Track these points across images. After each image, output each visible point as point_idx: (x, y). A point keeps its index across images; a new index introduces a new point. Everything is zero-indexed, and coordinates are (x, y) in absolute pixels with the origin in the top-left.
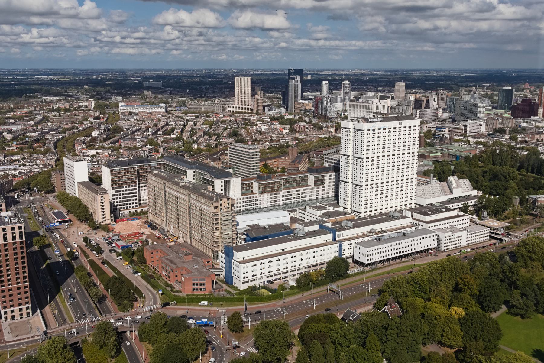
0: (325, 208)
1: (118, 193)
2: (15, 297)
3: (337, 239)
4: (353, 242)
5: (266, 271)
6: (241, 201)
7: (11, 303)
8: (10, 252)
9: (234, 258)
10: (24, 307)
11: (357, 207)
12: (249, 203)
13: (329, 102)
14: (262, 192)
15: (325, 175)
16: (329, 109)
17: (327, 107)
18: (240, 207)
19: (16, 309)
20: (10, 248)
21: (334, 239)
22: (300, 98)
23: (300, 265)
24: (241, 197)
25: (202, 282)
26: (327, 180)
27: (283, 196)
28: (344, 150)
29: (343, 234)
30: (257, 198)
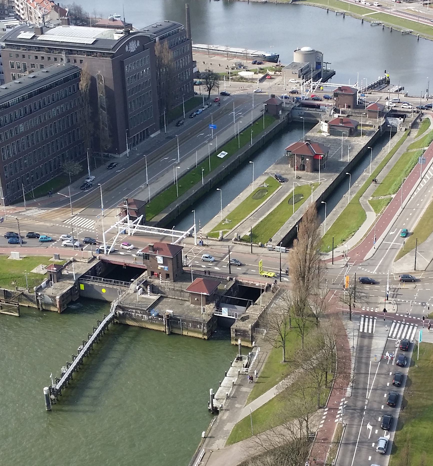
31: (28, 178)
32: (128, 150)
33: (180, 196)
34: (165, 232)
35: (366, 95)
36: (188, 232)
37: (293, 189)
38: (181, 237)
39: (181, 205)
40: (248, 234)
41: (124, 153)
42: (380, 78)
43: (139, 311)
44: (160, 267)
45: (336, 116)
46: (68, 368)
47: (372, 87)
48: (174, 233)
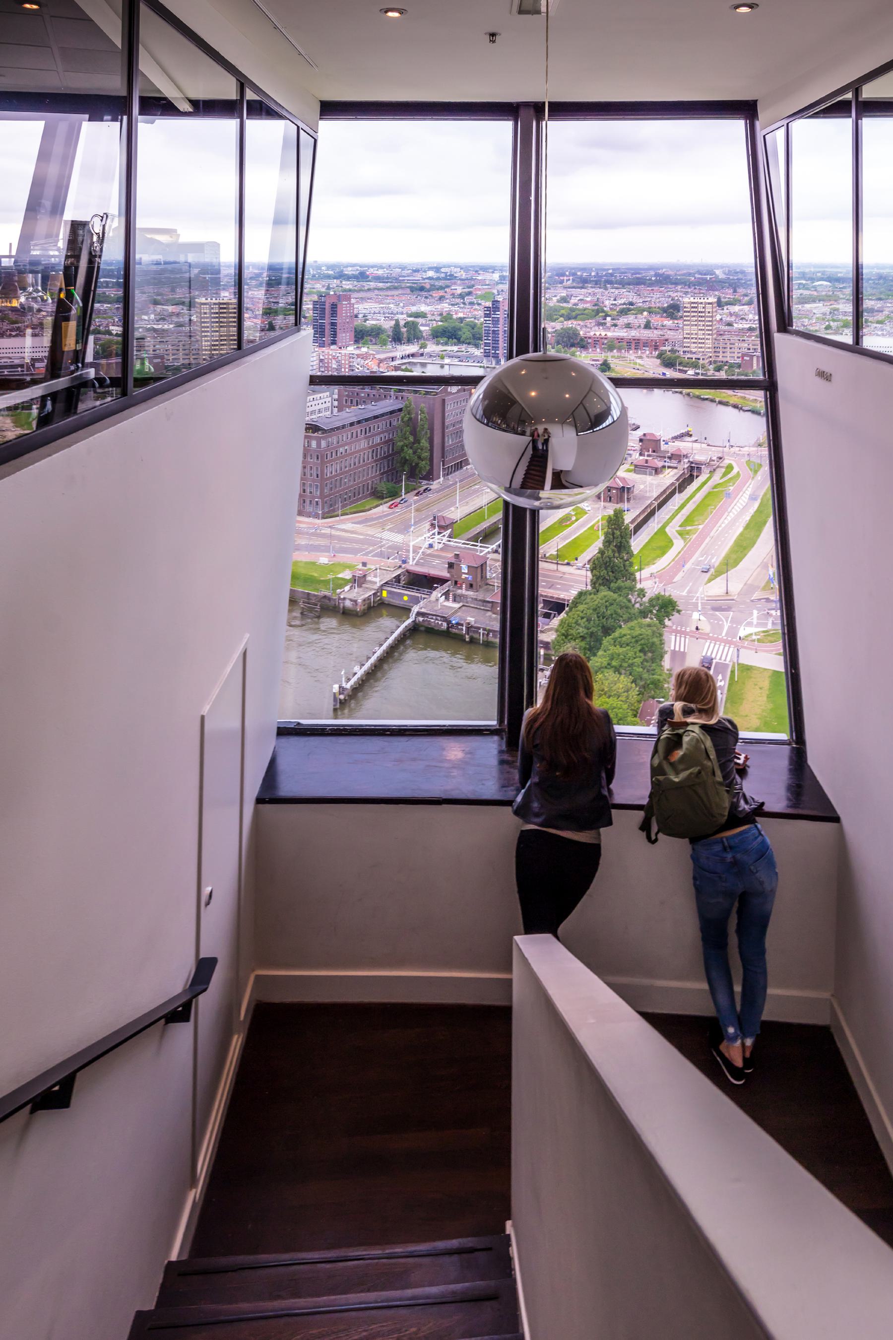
31: (346, 496)
32: (442, 479)
33: (488, 518)
34: (472, 545)
35: (669, 443)
37: (600, 517)
38: (487, 550)
39: (489, 527)
40: (555, 553)
41: (437, 481)
42: (683, 431)
43: (439, 618)
44: (464, 576)
45: (641, 458)
46: (361, 668)
47: (676, 438)
48: (481, 547)
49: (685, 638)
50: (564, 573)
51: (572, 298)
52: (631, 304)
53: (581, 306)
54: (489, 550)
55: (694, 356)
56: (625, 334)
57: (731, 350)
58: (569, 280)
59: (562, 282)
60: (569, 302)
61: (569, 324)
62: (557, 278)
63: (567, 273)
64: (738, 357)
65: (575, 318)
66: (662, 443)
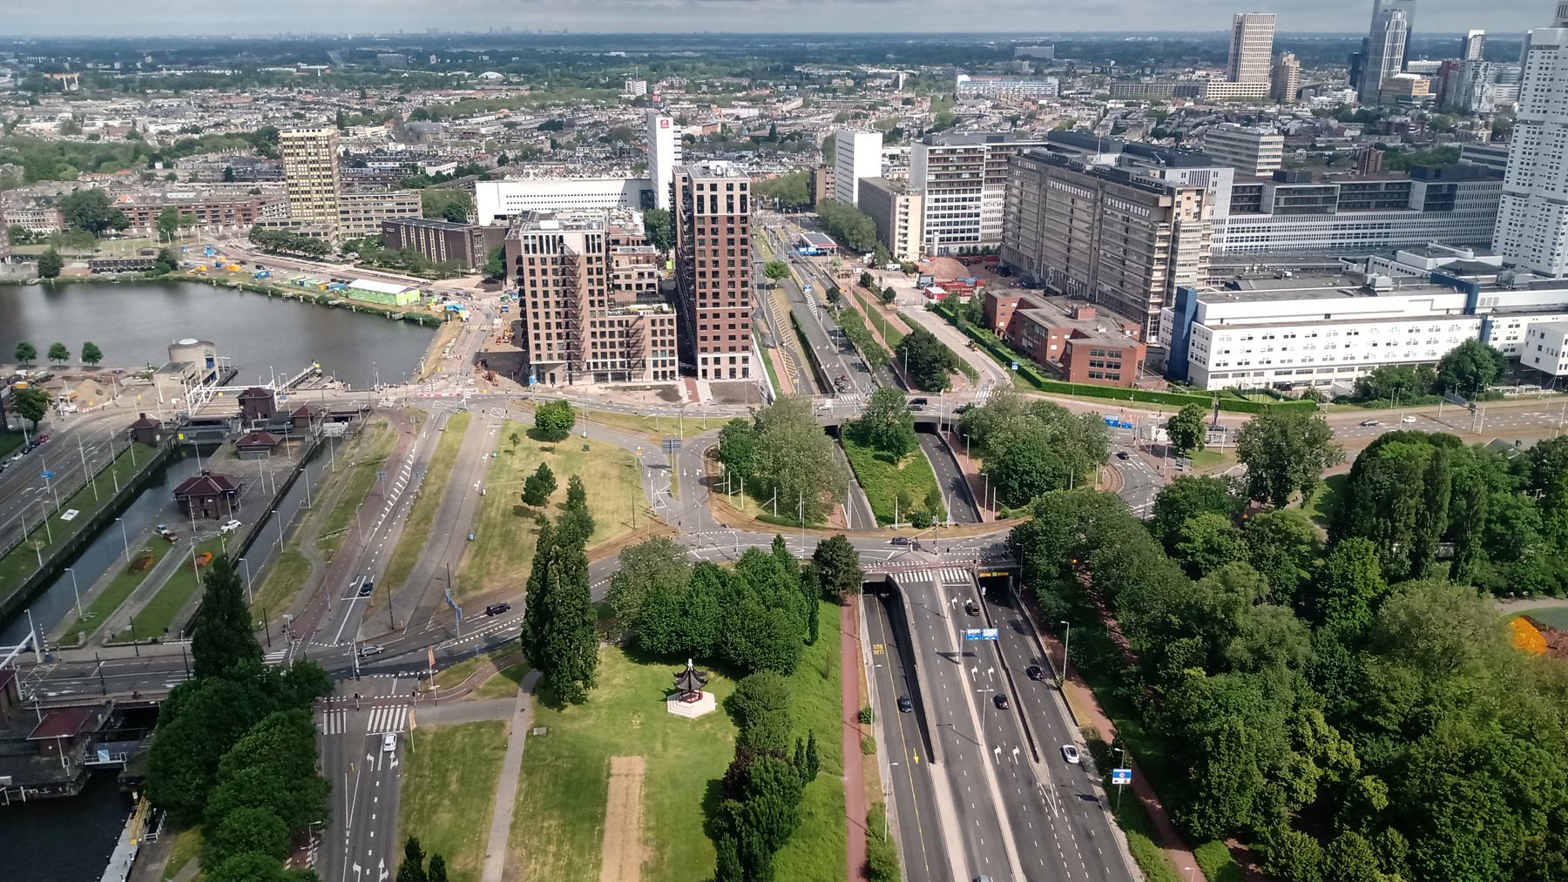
0: (1451, 254)
1: (941, 204)
2: (724, 333)
3: (1477, 311)
4: (1525, 321)
5: (1276, 358)
6: (1227, 226)
7: (717, 344)
8: (723, 236)
9: (1199, 318)
10: (739, 355)
11: (1544, 262)
12: (1245, 235)
13: (1482, 73)
14: (1284, 211)
15: (1459, 184)
16: (1478, 91)
17: (1473, 87)
18: (1221, 240)
19: (725, 356)
20: (722, 227)
21: (1469, 310)
22: (1398, 68)
23: (1366, 357)
24: (1228, 217)
25: (1115, 360)
26: (1463, 197)
27: (1336, 227)
28: (1527, 110)
29: (1496, 300)
30: (1266, 225)
36: (22, 645)
38: (10, 656)
45: (247, 431)
49: (342, 712)
50: (150, 658)
51: (86, 121)
52: (196, 130)
53: (105, 139)
54: (14, 654)
55: (310, 230)
56: (191, 195)
57: (367, 215)
58: (71, 81)
59: (58, 86)
60: (79, 132)
61: (88, 183)
62: (48, 76)
63: (67, 66)
64: (378, 226)
65: (96, 168)
66: (276, 397)
